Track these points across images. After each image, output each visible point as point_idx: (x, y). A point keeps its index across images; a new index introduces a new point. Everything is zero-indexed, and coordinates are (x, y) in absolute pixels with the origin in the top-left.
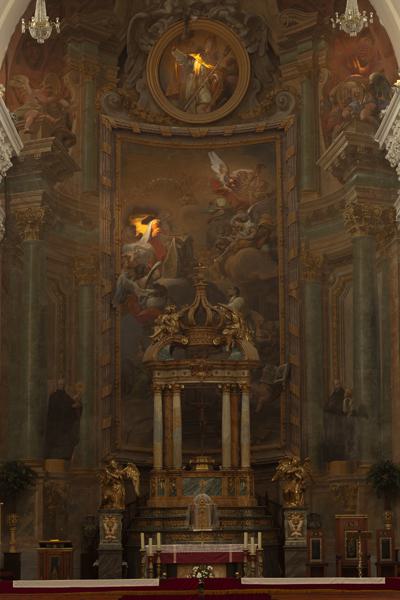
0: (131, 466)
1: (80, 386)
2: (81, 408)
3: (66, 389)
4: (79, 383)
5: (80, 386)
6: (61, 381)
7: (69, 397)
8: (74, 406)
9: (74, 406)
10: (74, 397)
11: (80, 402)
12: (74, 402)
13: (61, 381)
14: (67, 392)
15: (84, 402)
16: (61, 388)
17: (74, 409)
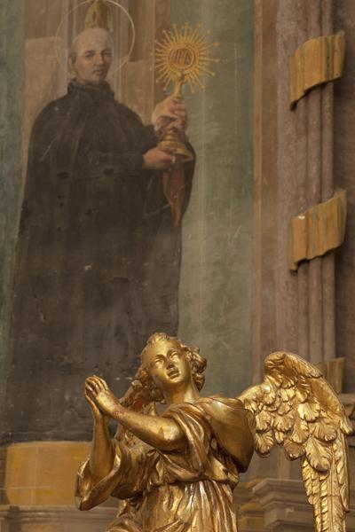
0: (289, 373)
1: (185, 56)
2: (186, 169)
3: (113, 76)
4: (177, 43)
5: (185, 56)
6: (91, 39)
7: (132, 117)
8: (154, 157)
9: (154, 157)
10: (154, 118)
11: (181, 136)
12: (150, 138)
13: (91, 39)
14: (119, 96)
15: (203, 133)
16: (88, 72)
17: (153, 174)
